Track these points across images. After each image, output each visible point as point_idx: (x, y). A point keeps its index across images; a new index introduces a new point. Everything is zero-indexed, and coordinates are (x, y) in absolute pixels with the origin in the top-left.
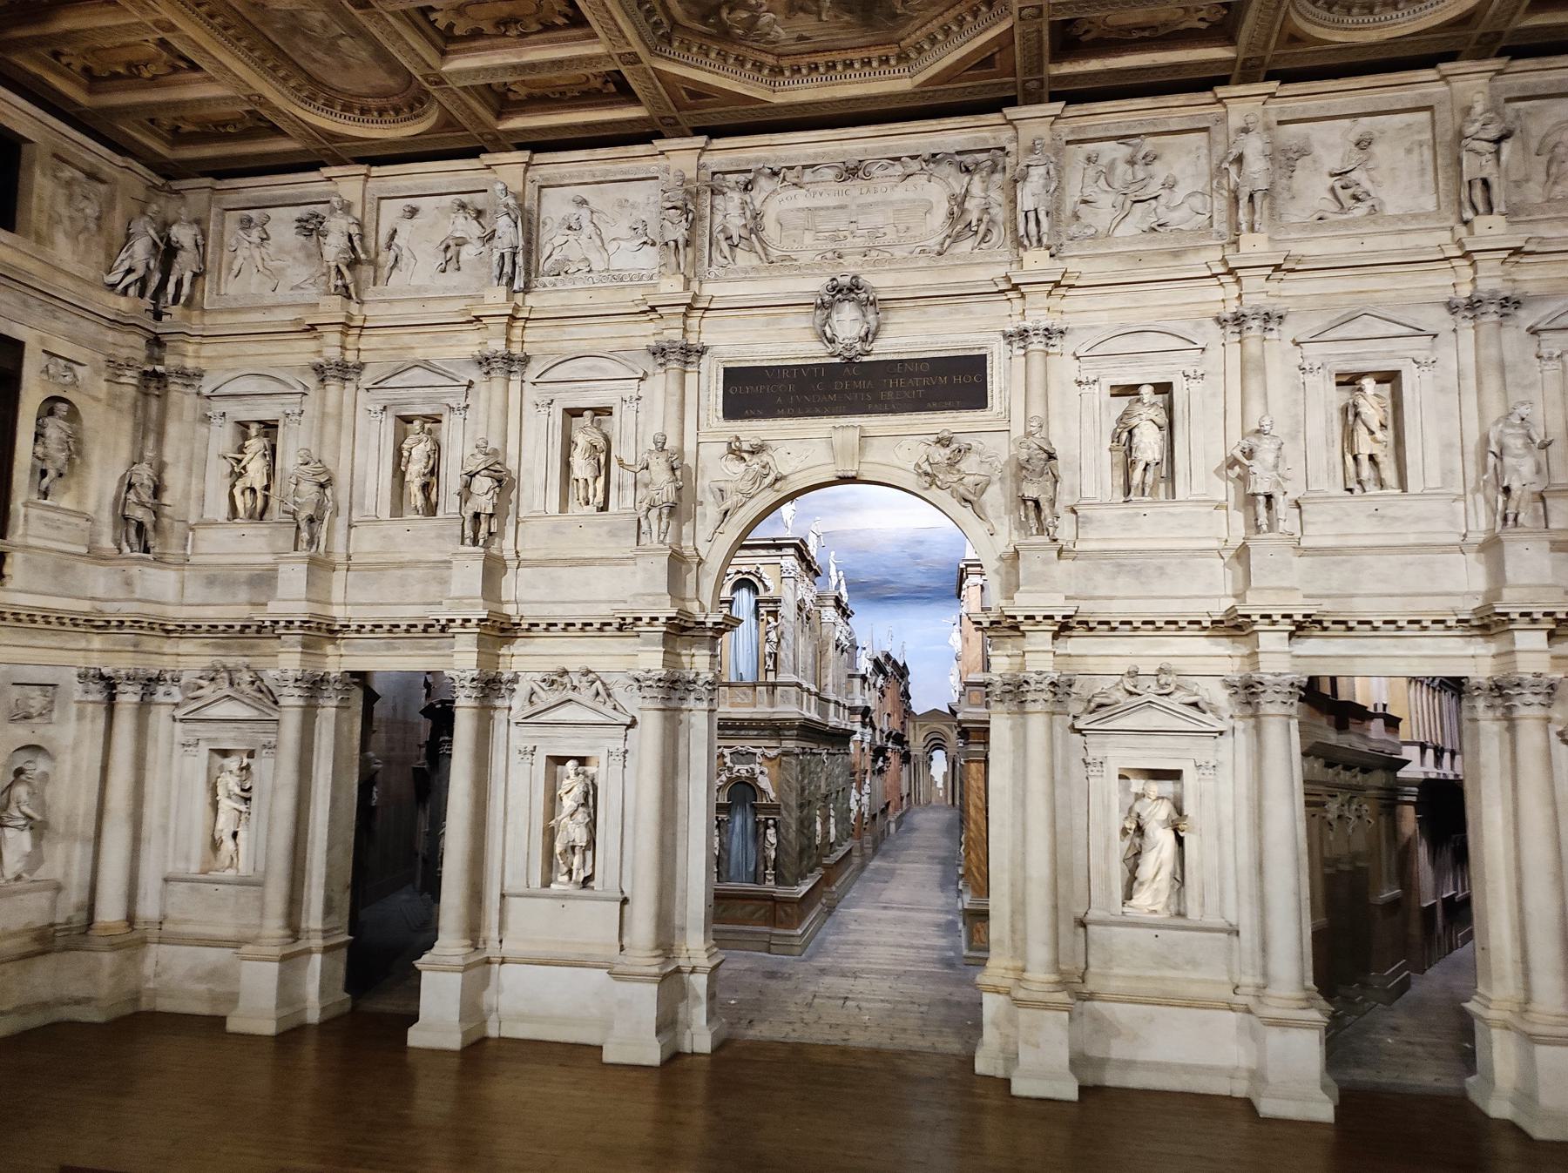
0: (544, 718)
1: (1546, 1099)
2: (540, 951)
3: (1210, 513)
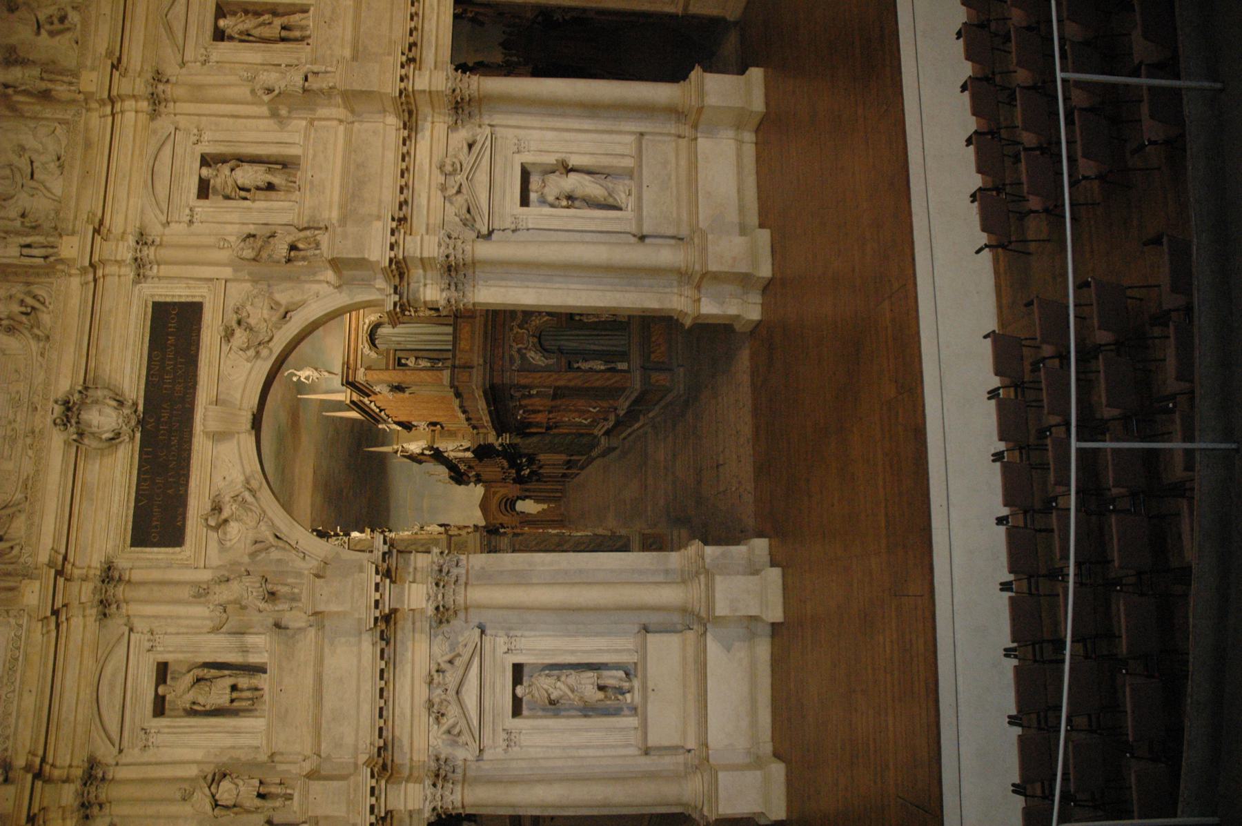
0: (475, 722)
2: (692, 708)
3: (316, 130)
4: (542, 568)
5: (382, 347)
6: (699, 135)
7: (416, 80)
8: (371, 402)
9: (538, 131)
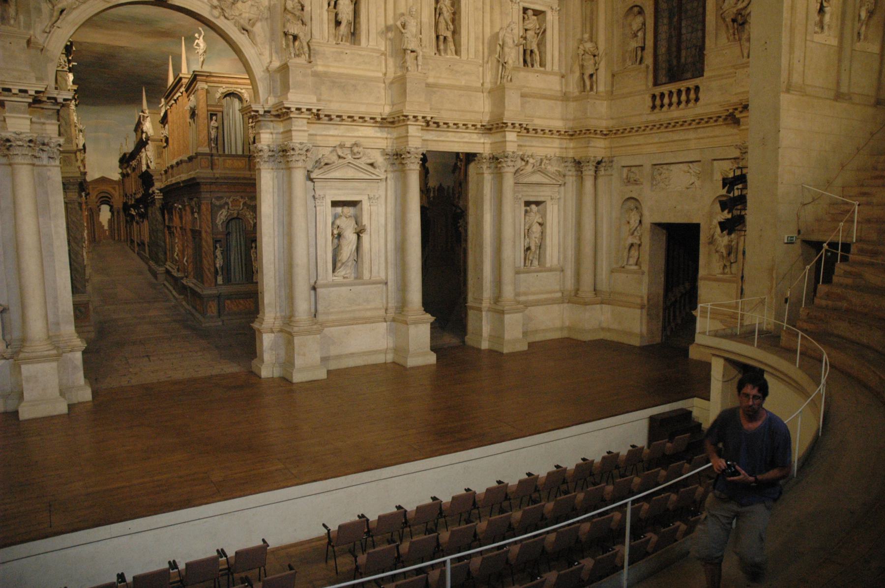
1: (508, 336)
3: (378, 57)
4: (52, 225)
5: (224, 101)
6: (388, 323)
7: (416, 127)
8: (182, 93)
9: (384, 211)
